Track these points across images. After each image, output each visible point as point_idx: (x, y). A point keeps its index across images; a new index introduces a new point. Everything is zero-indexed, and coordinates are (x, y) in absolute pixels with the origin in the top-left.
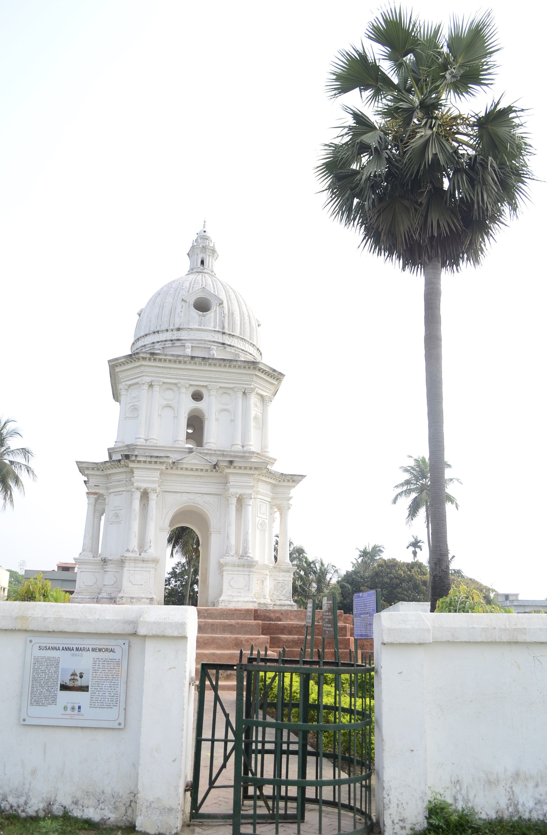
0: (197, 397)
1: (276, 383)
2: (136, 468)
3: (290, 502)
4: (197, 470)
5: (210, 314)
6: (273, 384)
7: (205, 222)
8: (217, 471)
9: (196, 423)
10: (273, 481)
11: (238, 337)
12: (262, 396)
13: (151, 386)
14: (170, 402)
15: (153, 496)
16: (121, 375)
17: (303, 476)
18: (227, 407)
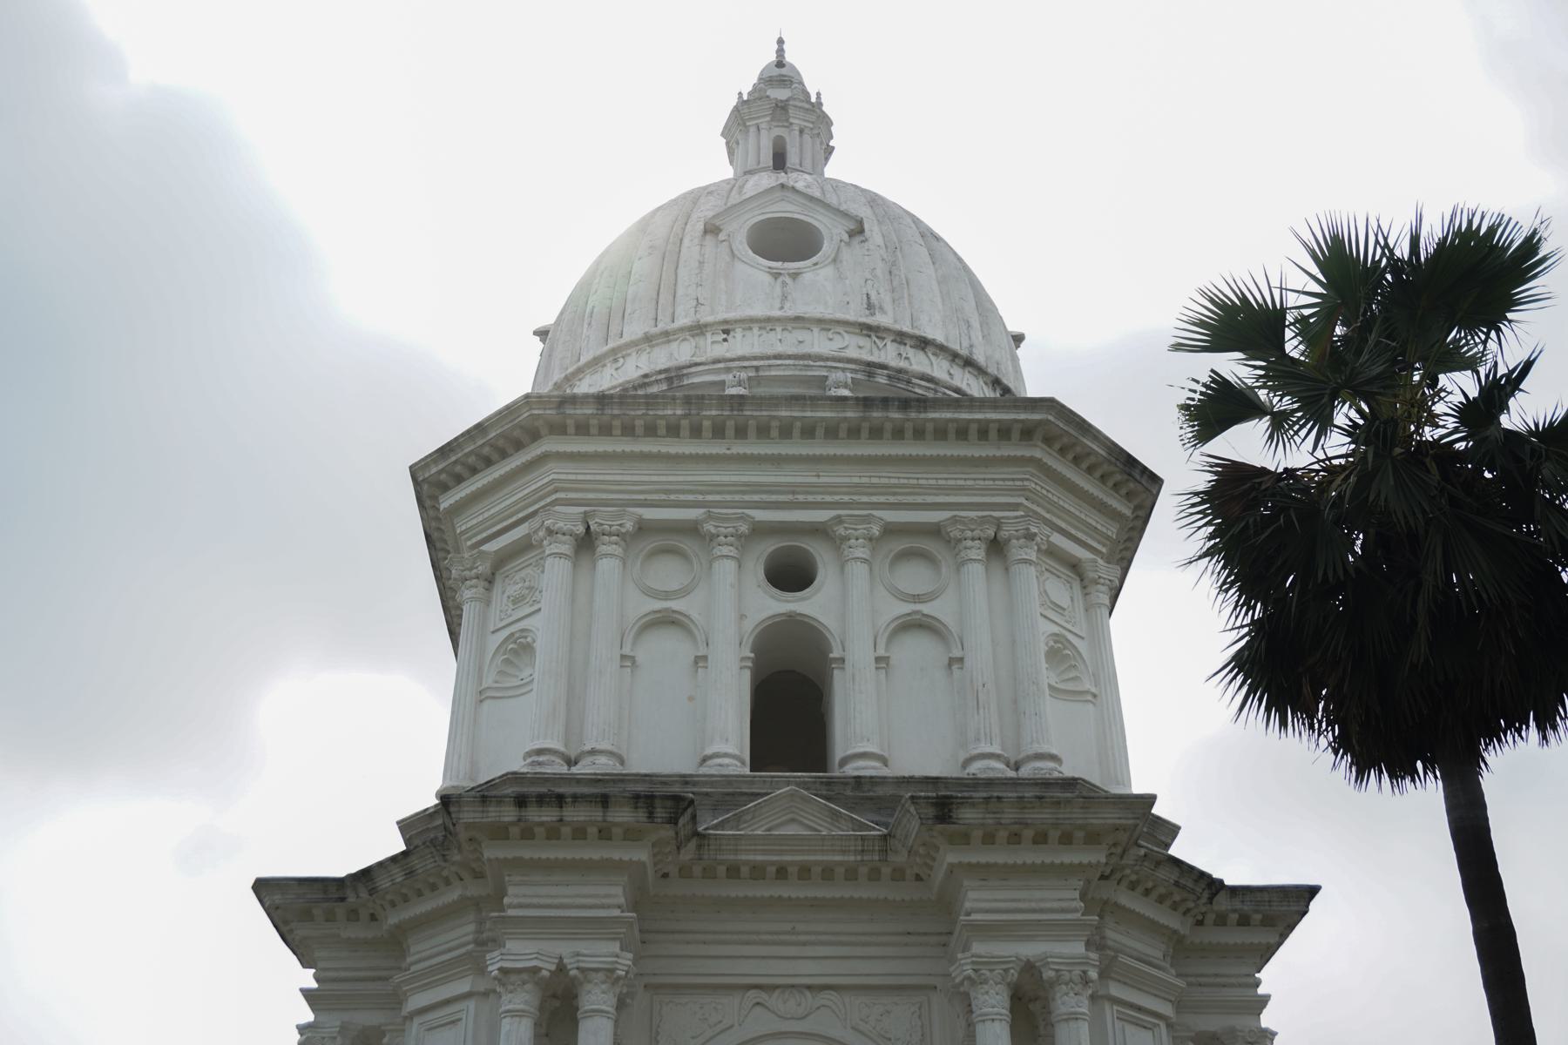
0: (791, 575)
2: (518, 864)
3: (1267, 1020)
4: (805, 872)
6: (1115, 515)
7: (781, 42)
9: (790, 704)
10: (1172, 921)
11: (942, 349)
13: (586, 543)
14: (674, 605)
15: (597, 998)
17: (1313, 891)
18: (925, 608)
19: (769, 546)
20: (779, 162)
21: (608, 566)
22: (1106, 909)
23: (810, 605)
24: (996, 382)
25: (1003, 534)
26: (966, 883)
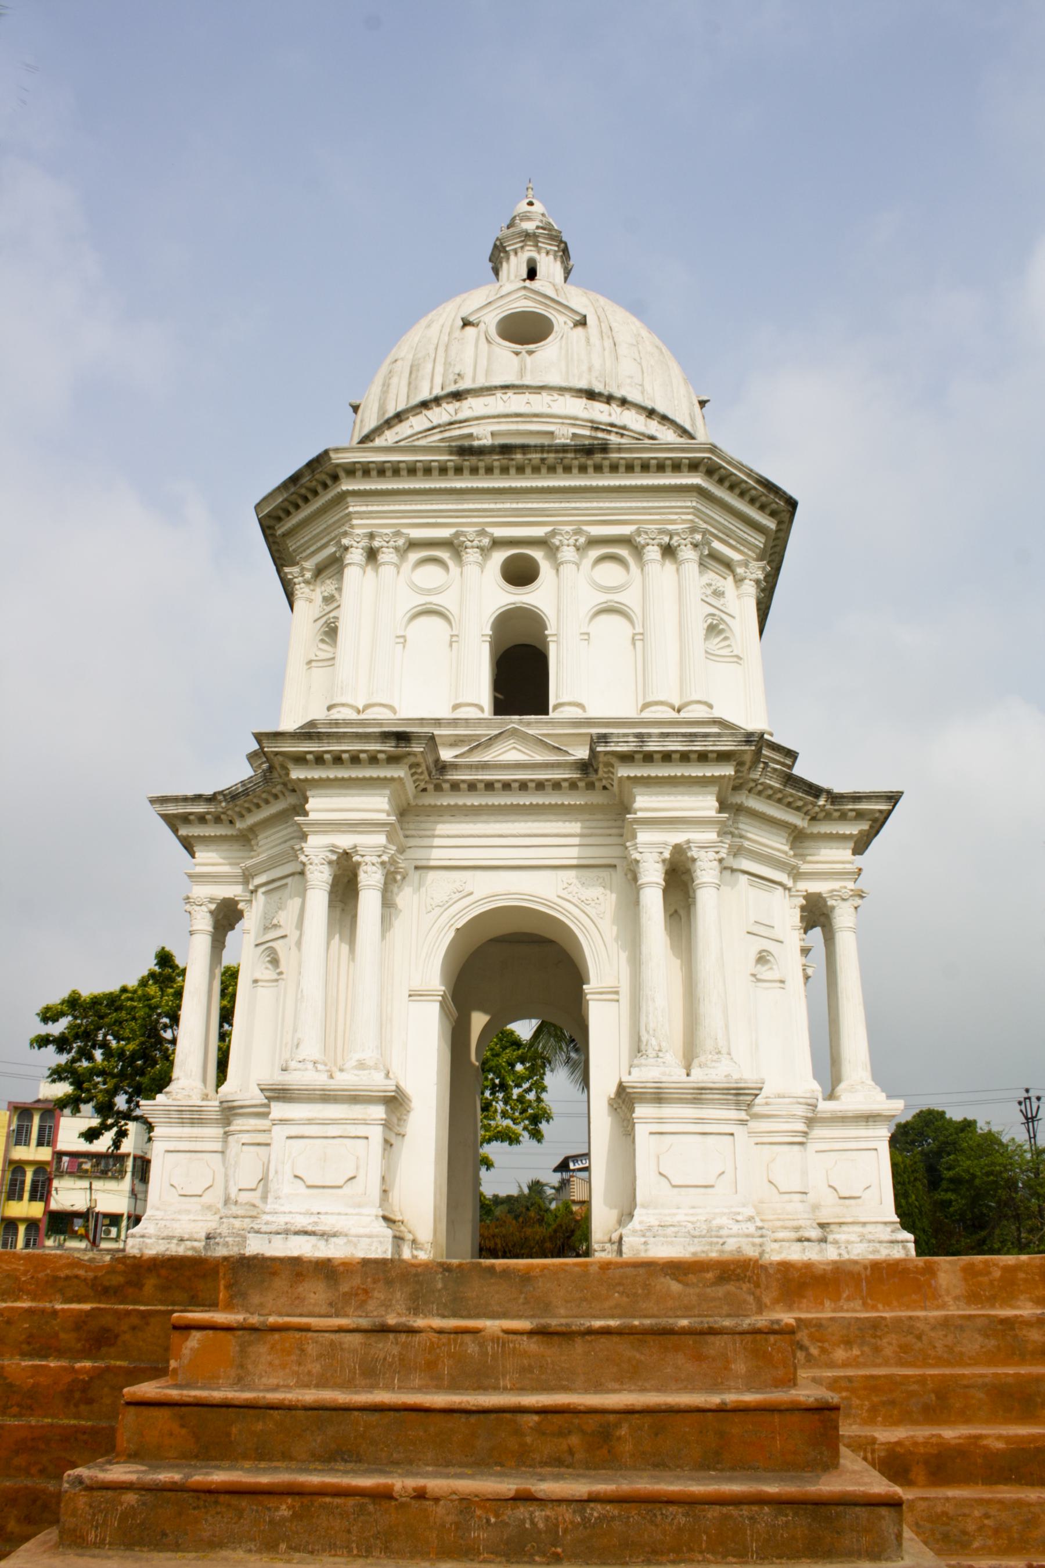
0: (520, 574)
1: (771, 524)
5: (548, 351)
8: (591, 786)
12: (728, 565)
13: (372, 554)
14: (436, 599)
16: (292, 545)
17: (893, 798)
19: (500, 556)
20: (532, 274)
21: (387, 571)
22: (739, 810)
23: (535, 597)
24: (684, 432)
25: (674, 542)
26: (634, 790)
